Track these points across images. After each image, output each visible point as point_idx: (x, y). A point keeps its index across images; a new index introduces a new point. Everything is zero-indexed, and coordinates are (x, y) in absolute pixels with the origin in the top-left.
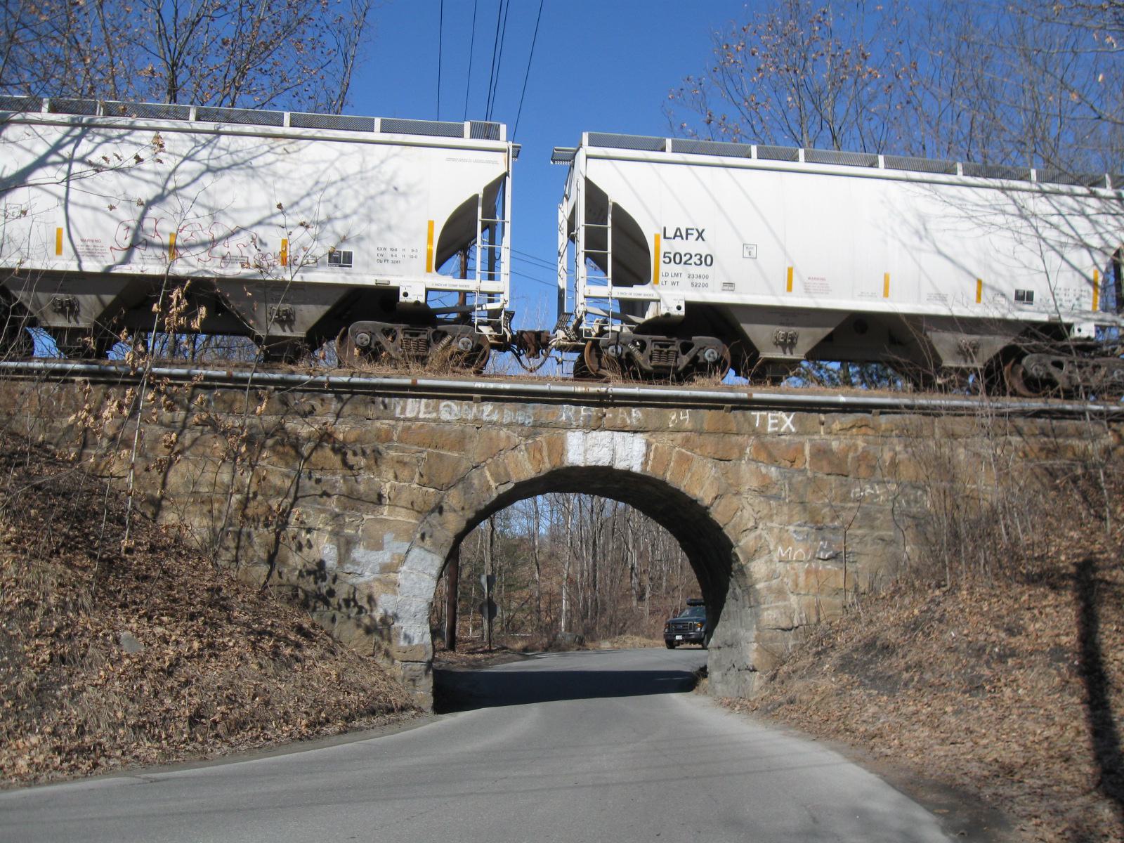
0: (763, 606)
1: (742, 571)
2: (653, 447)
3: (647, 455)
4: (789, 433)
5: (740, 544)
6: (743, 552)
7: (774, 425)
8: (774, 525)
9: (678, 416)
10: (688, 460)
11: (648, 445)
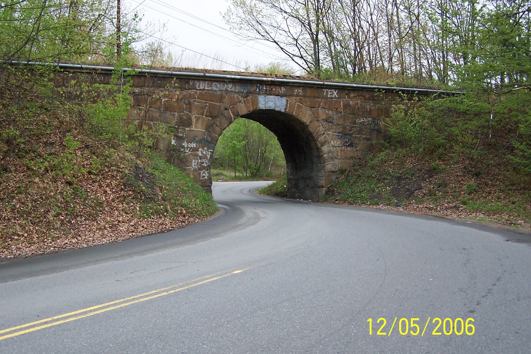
0: (326, 163)
1: (318, 149)
2: (289, 102)
3: (287, 105)
4: (335, 98)
5: (319, 140)
6: (320, 143)
7: (330, 95)
8: (330, 133)
9: (298, 90)
10: (301, 107)
11: (287, 101)
